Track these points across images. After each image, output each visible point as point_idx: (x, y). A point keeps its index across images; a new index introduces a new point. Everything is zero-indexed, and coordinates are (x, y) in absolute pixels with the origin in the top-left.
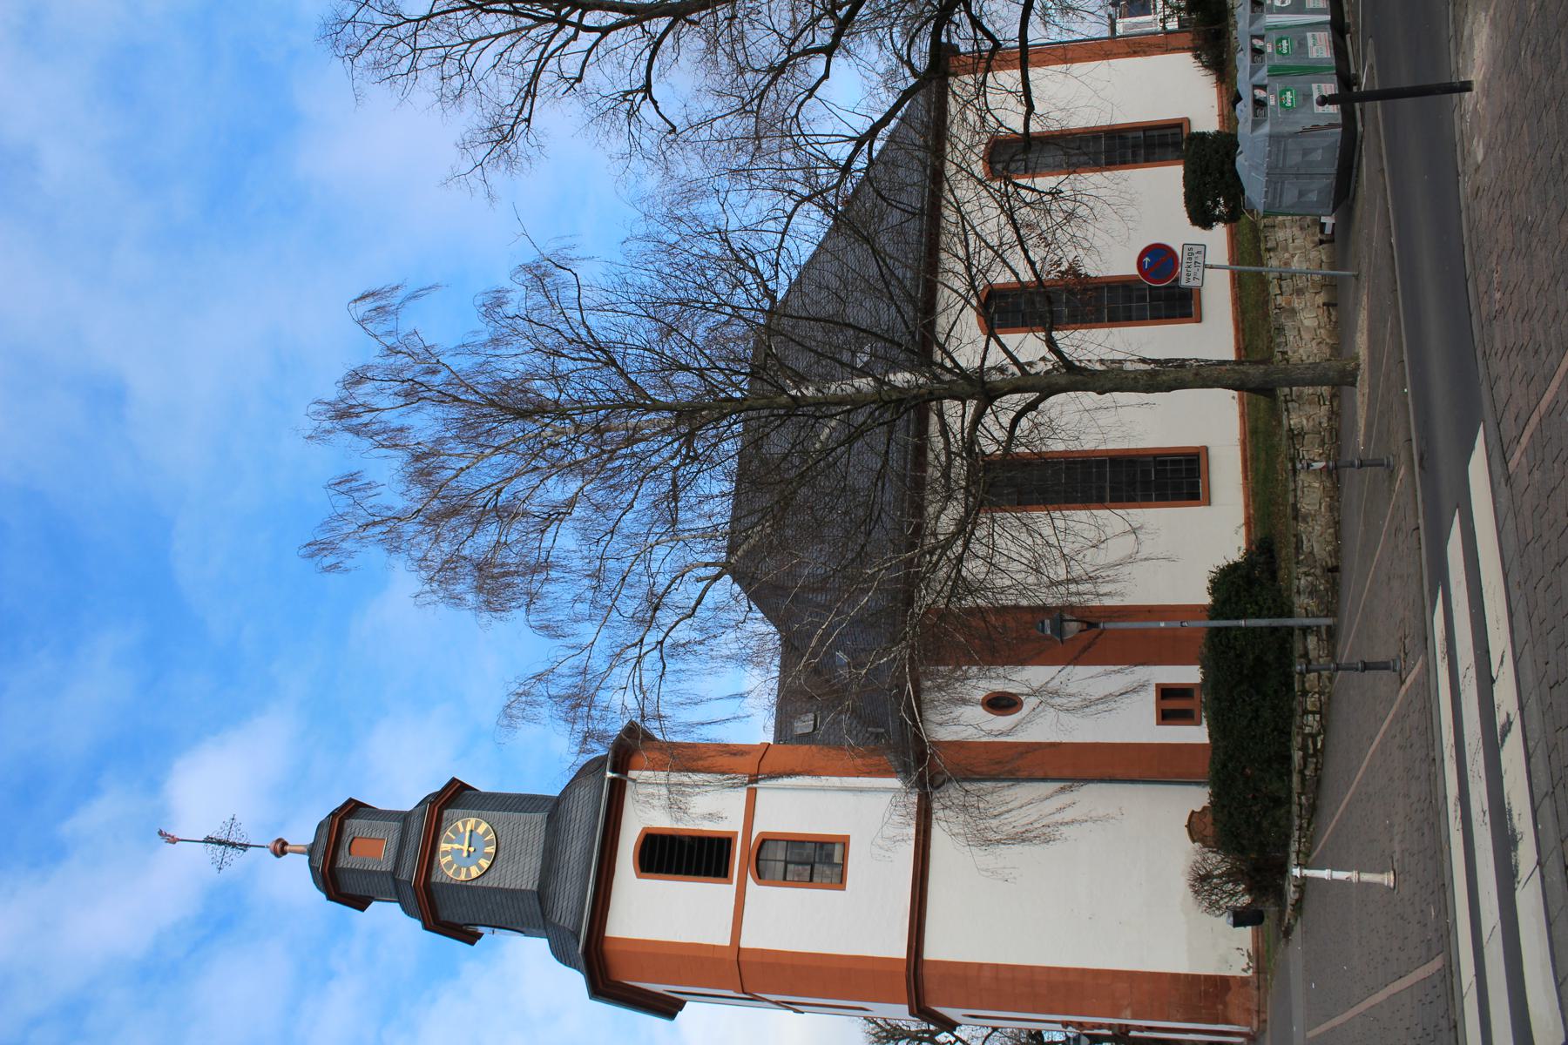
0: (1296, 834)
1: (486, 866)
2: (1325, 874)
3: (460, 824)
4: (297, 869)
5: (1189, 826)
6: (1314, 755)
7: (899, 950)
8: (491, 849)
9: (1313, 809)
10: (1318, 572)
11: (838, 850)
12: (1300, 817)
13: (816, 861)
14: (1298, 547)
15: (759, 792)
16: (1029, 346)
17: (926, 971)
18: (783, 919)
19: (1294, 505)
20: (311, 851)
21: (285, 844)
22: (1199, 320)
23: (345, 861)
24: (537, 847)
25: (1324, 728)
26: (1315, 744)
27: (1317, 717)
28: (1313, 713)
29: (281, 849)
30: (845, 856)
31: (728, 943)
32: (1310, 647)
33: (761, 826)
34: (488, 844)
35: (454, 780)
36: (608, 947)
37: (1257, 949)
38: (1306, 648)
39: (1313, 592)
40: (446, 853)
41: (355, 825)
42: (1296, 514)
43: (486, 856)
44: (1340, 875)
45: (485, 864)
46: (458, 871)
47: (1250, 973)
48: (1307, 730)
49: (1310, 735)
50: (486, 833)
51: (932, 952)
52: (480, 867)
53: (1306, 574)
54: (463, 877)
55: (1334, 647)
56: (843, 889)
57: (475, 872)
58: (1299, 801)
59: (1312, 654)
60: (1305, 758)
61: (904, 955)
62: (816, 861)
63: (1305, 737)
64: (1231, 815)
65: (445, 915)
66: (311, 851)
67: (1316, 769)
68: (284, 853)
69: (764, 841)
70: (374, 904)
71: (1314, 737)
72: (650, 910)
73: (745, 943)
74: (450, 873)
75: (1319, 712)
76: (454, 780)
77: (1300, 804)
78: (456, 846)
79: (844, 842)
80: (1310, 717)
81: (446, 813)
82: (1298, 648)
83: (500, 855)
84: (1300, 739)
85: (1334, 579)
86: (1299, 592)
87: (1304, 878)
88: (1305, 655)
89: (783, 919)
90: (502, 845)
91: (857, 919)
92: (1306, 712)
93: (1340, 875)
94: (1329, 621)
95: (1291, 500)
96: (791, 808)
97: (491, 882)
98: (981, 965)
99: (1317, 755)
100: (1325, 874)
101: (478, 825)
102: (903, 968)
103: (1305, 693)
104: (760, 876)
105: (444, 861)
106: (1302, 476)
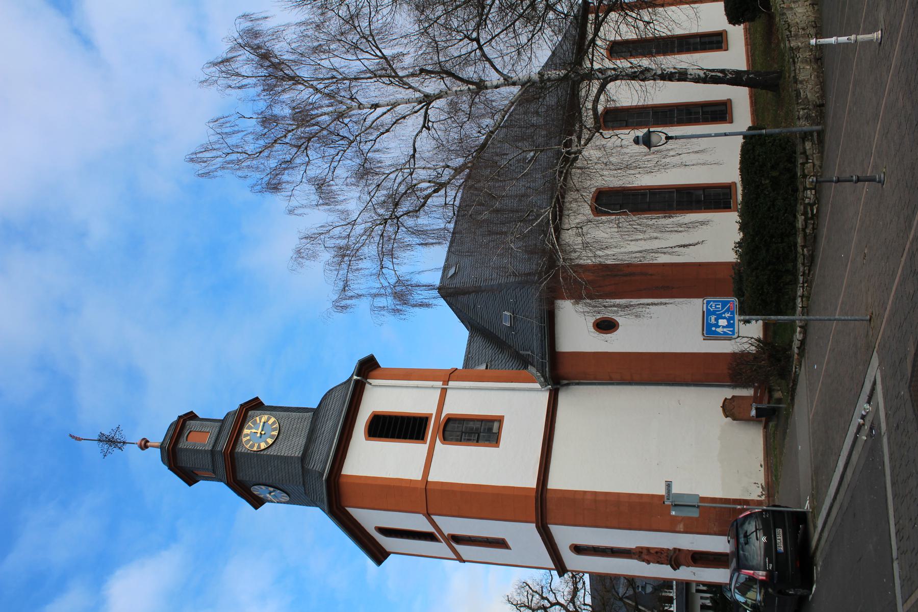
0: (801, 279)
1: (270, 442)
2: (832, 40)
3: (258, 419)
4: (155, 454)
5: (723, 407)
6: (812, 218)
7: (530, 481)
8: (275, 433)
9: (812, 259)
10: (811, 107)
11: (496, 425)
12: (803, 264)
13: (481, 431)
14: (798, 95)
15: (449, 392)
16: (623, 64)
17: (549, 495)
18: (458, 465)
19: (795, 77)
20: (161, 447)
21: (147, 441)
22: (727, 50)
23: (183, 444)
24: (305, 433)
25: (818, 200)
26: (812, 211)
27: (813, 192)
28: (811, 189)
29: (144, 445)
30: (500, 428)
31: (420, 478)
32: (807, 148)
33: (448, 410)
34: (274, 430)
35: (257, 398)
36: (342, 480)
37: (767, 483)
38: (804, 148)
39: (808, 117)
40: (247, 435)
41: (192, 424)
42: (796, 81)
43: (272, 437)
44: (843, 39)
45: (270, 441)
46: (253, 446)
47: (763, 498)
48: (807, 201)
49: (809, 204)
50: (274, 423)
51: (554, 483)
52: (266, 442)
53: (803, 109)
54: (255, 449)
55: (823, 147)
56: (498, 447)
57: (263, 446)
58: (802, 251)
59: (808, 152)
60: (806, 220)
61: (534, 486)
62: (481, 431)
63: (806, 206)
64: (757, 277)
65: (241, 476)
66: (161, 447)
67: (813, 229)
68: (146, 447)
69: (450, 420)
70: (201, 482)
71: (812, 205)
72: (370, 459)
73: (431, 478)
74: (247, 447)
75: (814, 189)
76: (257, 398)
77: (803, 254)
78: (254, 431)
79: (500, 420)
80: (809, 192)
81: (250, 413)
82: (799, 149)
83: (280, 437)
84: (802, 207)
85: (821, 111)
86: (799, 118)
87: (820, 47)
88: (804, 152)
89: (458, 465)
90: (282, 431)
91: (506, 466)
92: (805, 189)
93: (843, 39)
94: (819, 128)
95: (793, 75)
96: (467, 401)
97: (271, 452)
98: (585, 492)
99: (814, 219)
100: (832, 40)
101: (269, 419)
102: (534, 494)
103: (805, 176)
104: (445, 439)
105: (244, 439)
106: (798, 65)
